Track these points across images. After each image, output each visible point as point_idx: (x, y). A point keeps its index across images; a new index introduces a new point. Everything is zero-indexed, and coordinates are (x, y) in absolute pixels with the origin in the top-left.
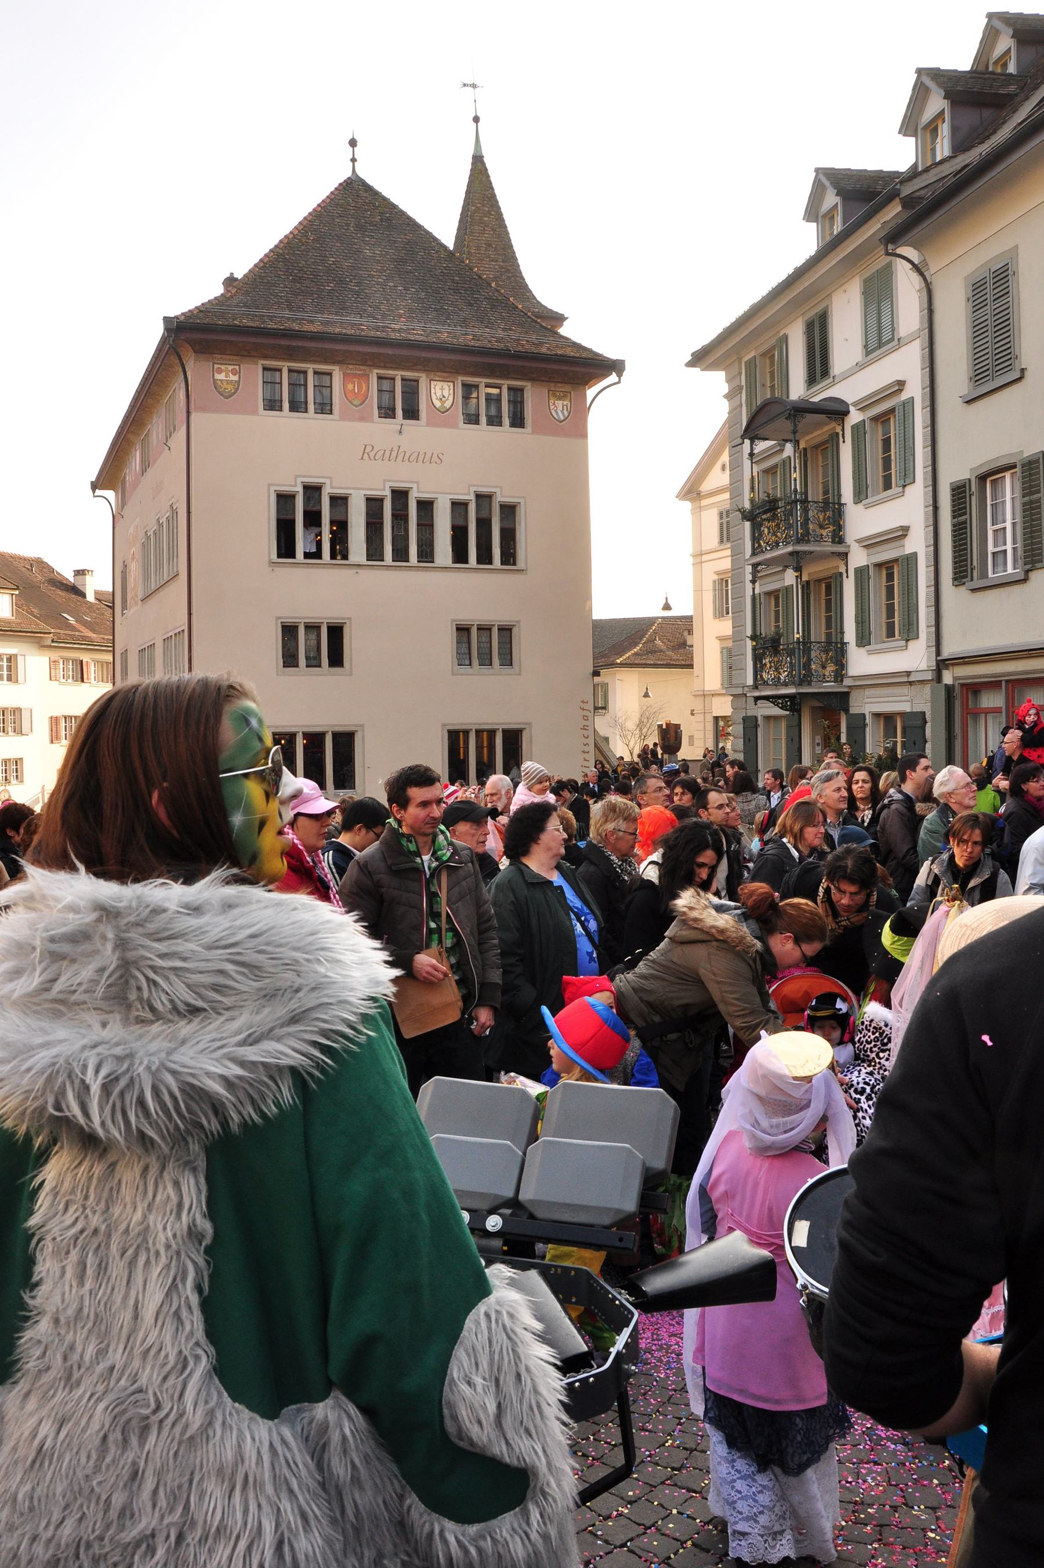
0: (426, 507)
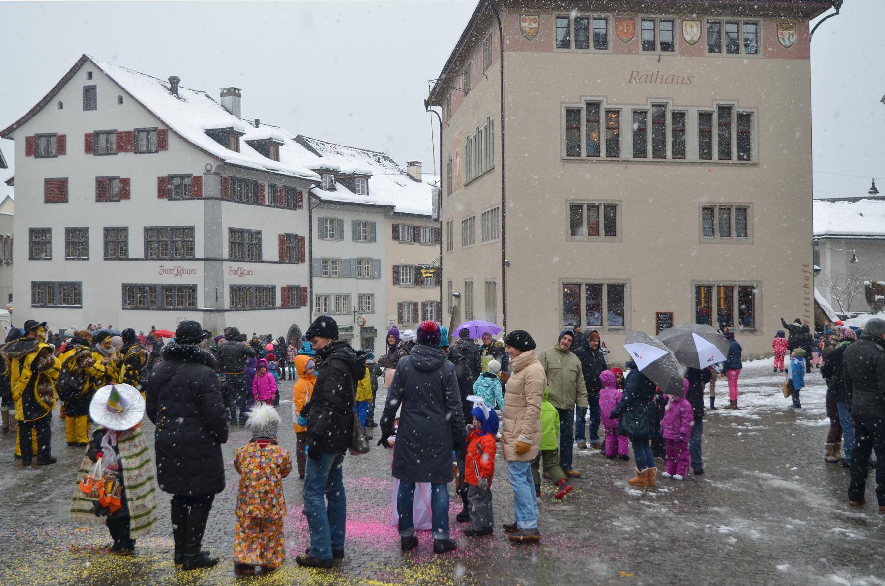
0: (679, 117)
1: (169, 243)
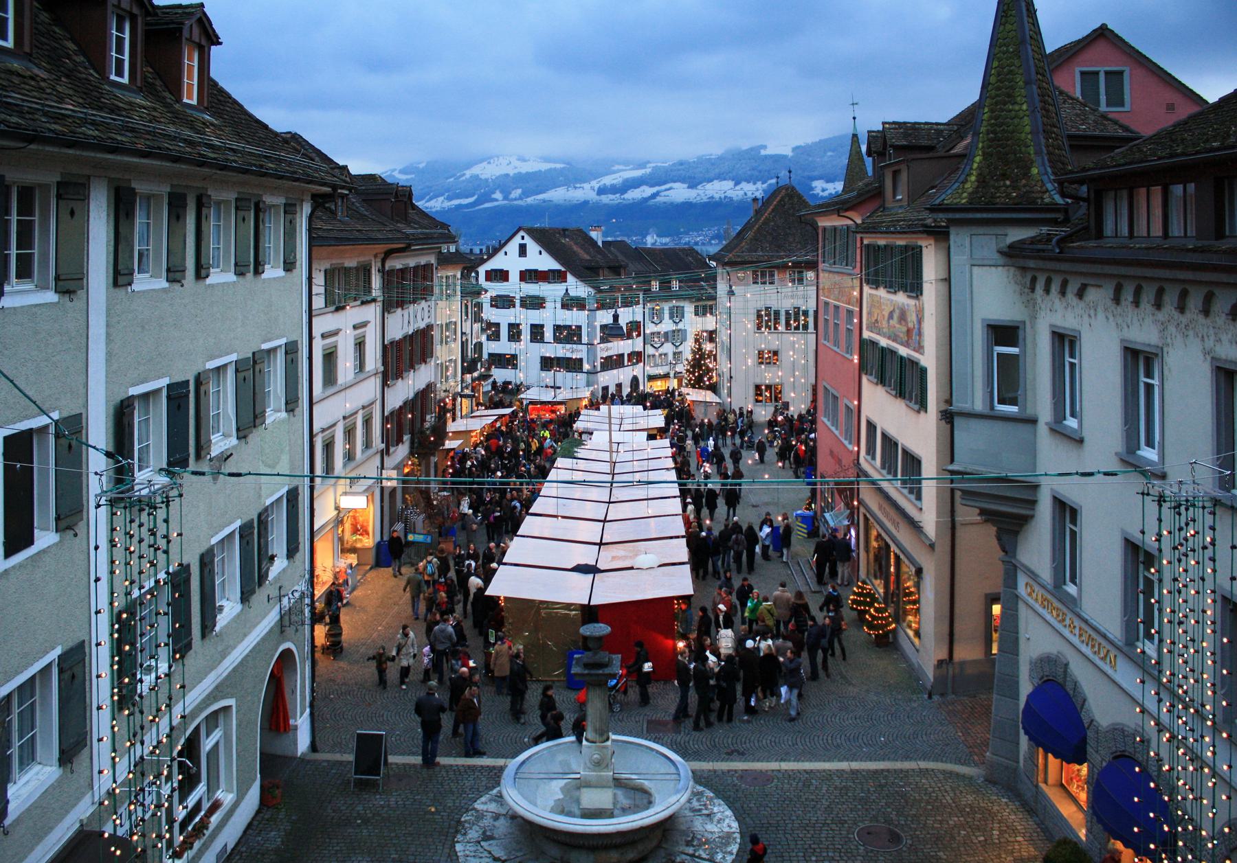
1: (567, 334)
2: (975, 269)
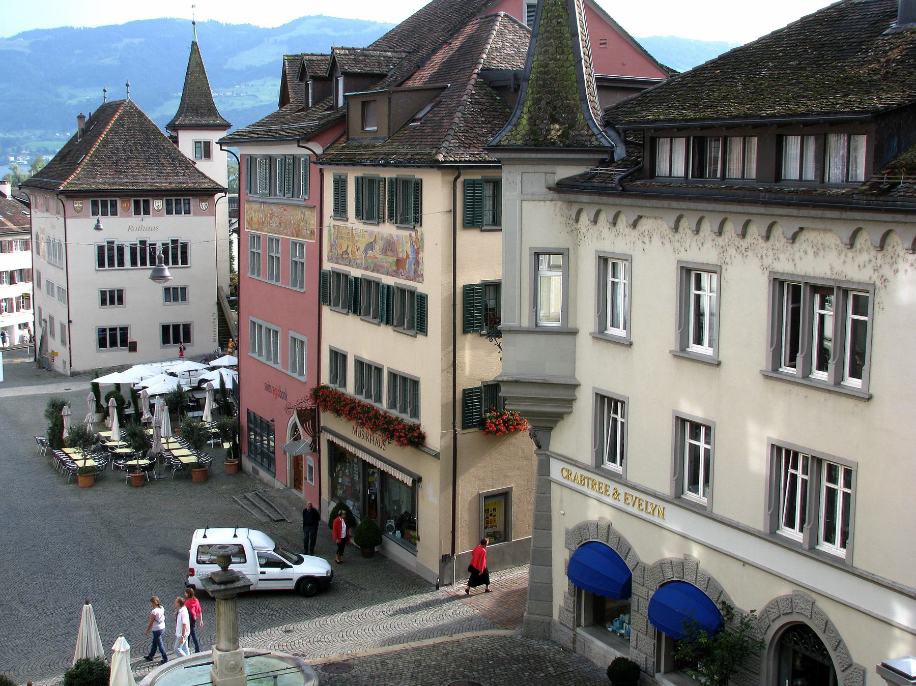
2: (525, 203)
